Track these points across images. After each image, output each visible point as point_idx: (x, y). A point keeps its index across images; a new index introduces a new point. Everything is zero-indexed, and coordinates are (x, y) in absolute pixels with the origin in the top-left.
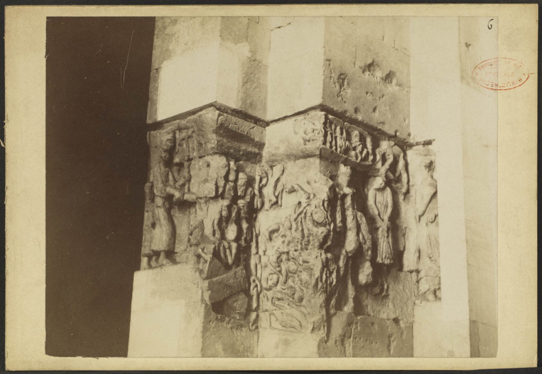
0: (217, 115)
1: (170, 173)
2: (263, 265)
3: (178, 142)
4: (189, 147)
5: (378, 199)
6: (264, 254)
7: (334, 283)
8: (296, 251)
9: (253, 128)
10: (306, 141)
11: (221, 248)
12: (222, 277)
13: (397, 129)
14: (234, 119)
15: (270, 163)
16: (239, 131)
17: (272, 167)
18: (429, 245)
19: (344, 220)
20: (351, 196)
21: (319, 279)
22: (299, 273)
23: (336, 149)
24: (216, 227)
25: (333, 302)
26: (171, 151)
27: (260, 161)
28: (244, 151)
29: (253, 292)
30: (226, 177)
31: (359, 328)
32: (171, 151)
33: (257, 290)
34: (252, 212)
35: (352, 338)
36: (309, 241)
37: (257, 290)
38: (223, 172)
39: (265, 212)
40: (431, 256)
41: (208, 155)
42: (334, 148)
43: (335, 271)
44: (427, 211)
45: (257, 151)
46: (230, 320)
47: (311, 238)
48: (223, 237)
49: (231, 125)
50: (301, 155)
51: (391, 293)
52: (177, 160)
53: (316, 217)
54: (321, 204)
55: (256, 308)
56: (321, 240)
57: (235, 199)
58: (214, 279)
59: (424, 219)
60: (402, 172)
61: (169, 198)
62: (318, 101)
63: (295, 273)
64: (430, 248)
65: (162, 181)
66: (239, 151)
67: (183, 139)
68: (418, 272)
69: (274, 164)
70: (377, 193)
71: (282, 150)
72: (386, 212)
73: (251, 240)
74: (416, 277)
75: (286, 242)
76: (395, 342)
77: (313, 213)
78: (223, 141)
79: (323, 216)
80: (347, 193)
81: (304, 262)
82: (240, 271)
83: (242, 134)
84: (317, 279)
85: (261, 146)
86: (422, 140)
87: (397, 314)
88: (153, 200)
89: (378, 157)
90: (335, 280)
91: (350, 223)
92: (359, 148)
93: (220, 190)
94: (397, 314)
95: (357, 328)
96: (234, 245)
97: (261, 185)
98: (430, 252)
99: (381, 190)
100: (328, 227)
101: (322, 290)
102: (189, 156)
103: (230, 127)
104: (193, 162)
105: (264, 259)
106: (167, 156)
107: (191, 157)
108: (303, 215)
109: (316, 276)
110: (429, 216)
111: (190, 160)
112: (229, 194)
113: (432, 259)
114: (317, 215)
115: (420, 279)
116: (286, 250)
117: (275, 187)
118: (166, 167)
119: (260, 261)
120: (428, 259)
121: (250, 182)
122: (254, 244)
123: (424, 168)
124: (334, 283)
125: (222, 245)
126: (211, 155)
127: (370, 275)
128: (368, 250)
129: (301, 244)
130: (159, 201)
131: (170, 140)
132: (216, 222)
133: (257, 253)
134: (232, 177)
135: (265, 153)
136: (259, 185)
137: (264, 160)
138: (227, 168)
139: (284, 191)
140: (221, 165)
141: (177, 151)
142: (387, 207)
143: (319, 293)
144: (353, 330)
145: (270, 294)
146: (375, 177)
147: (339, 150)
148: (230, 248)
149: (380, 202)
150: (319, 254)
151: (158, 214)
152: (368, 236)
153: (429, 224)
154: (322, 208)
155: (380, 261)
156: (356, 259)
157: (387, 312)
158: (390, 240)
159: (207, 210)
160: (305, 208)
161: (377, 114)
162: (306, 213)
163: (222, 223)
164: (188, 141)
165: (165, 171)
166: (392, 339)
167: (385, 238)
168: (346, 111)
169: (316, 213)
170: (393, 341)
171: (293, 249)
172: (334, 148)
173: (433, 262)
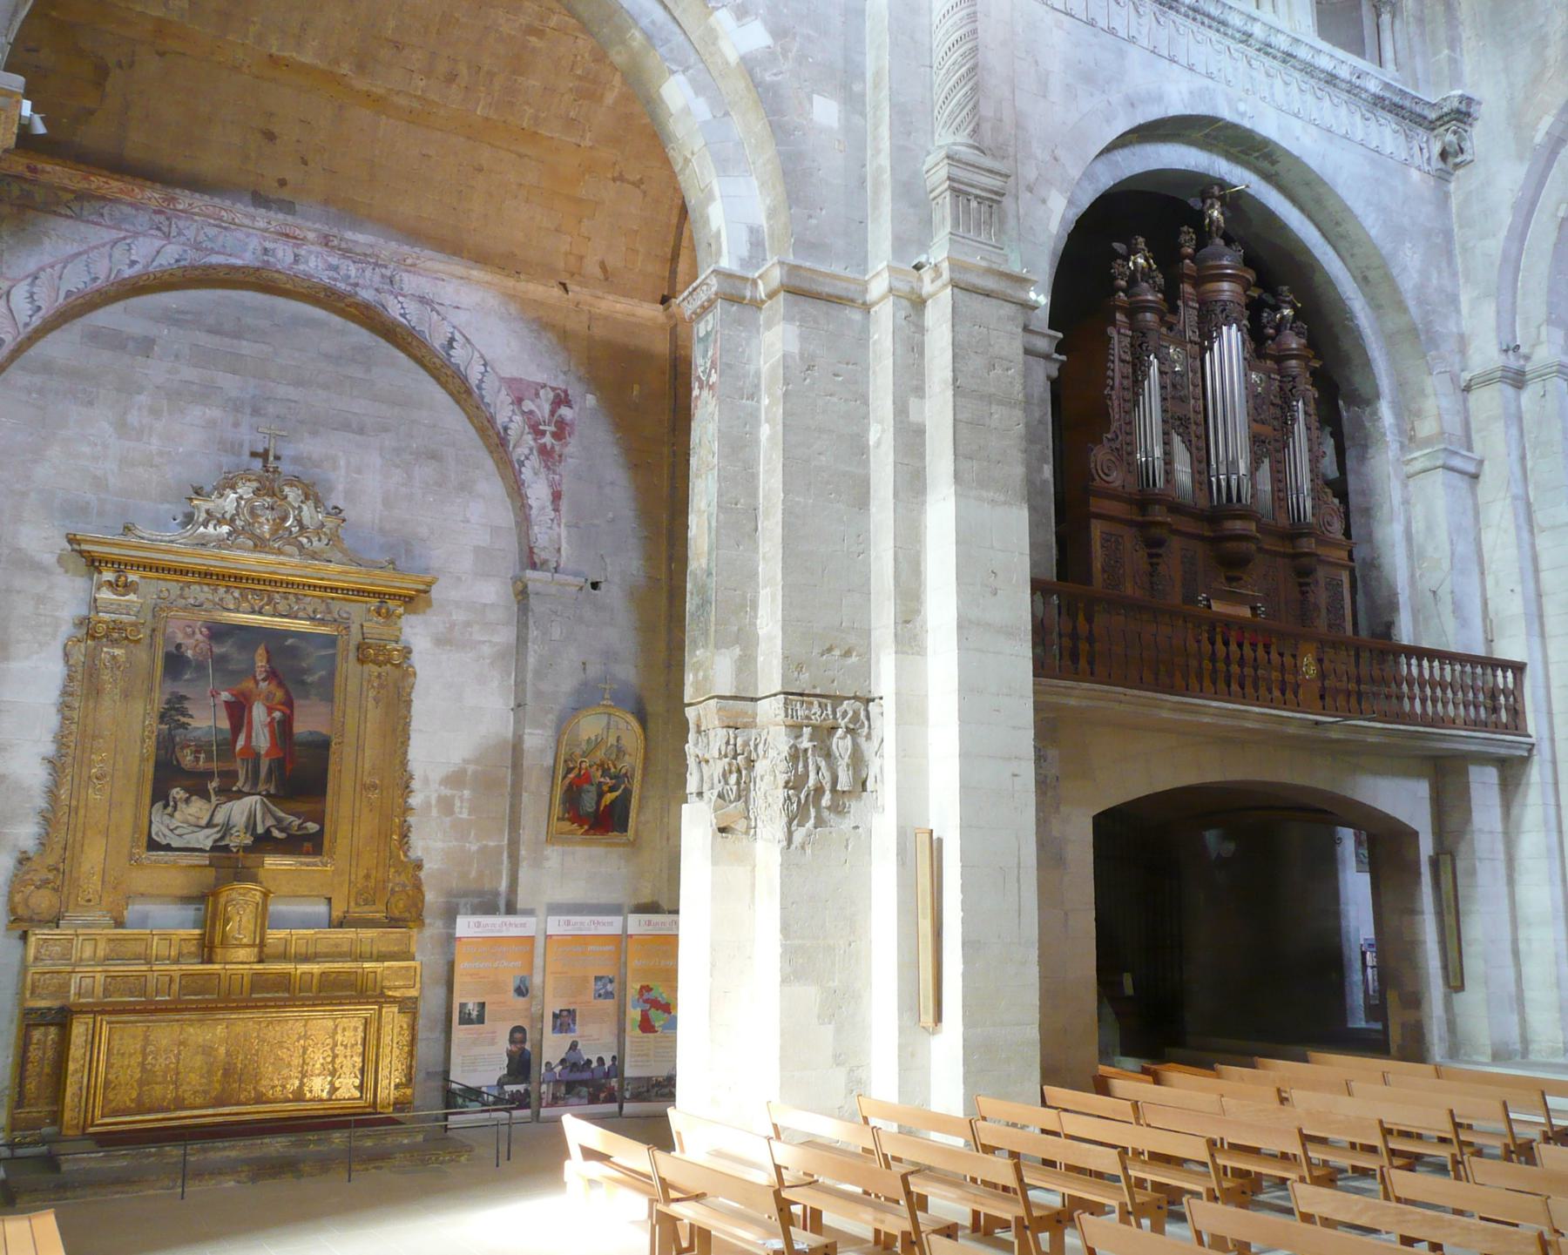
5: (841, 744)
19: (806, 766)
30: (728, 743)
34: (751, 763)
57: (735, 757)
62: (778, 689)
82: (740, 804)
91: (812, 768)
99: (844, 737)
112: (731, 754)
121: (746, 744)
152: (827, 775)
156: (819, 790)
157: (846, 824)
163: (725, 776)
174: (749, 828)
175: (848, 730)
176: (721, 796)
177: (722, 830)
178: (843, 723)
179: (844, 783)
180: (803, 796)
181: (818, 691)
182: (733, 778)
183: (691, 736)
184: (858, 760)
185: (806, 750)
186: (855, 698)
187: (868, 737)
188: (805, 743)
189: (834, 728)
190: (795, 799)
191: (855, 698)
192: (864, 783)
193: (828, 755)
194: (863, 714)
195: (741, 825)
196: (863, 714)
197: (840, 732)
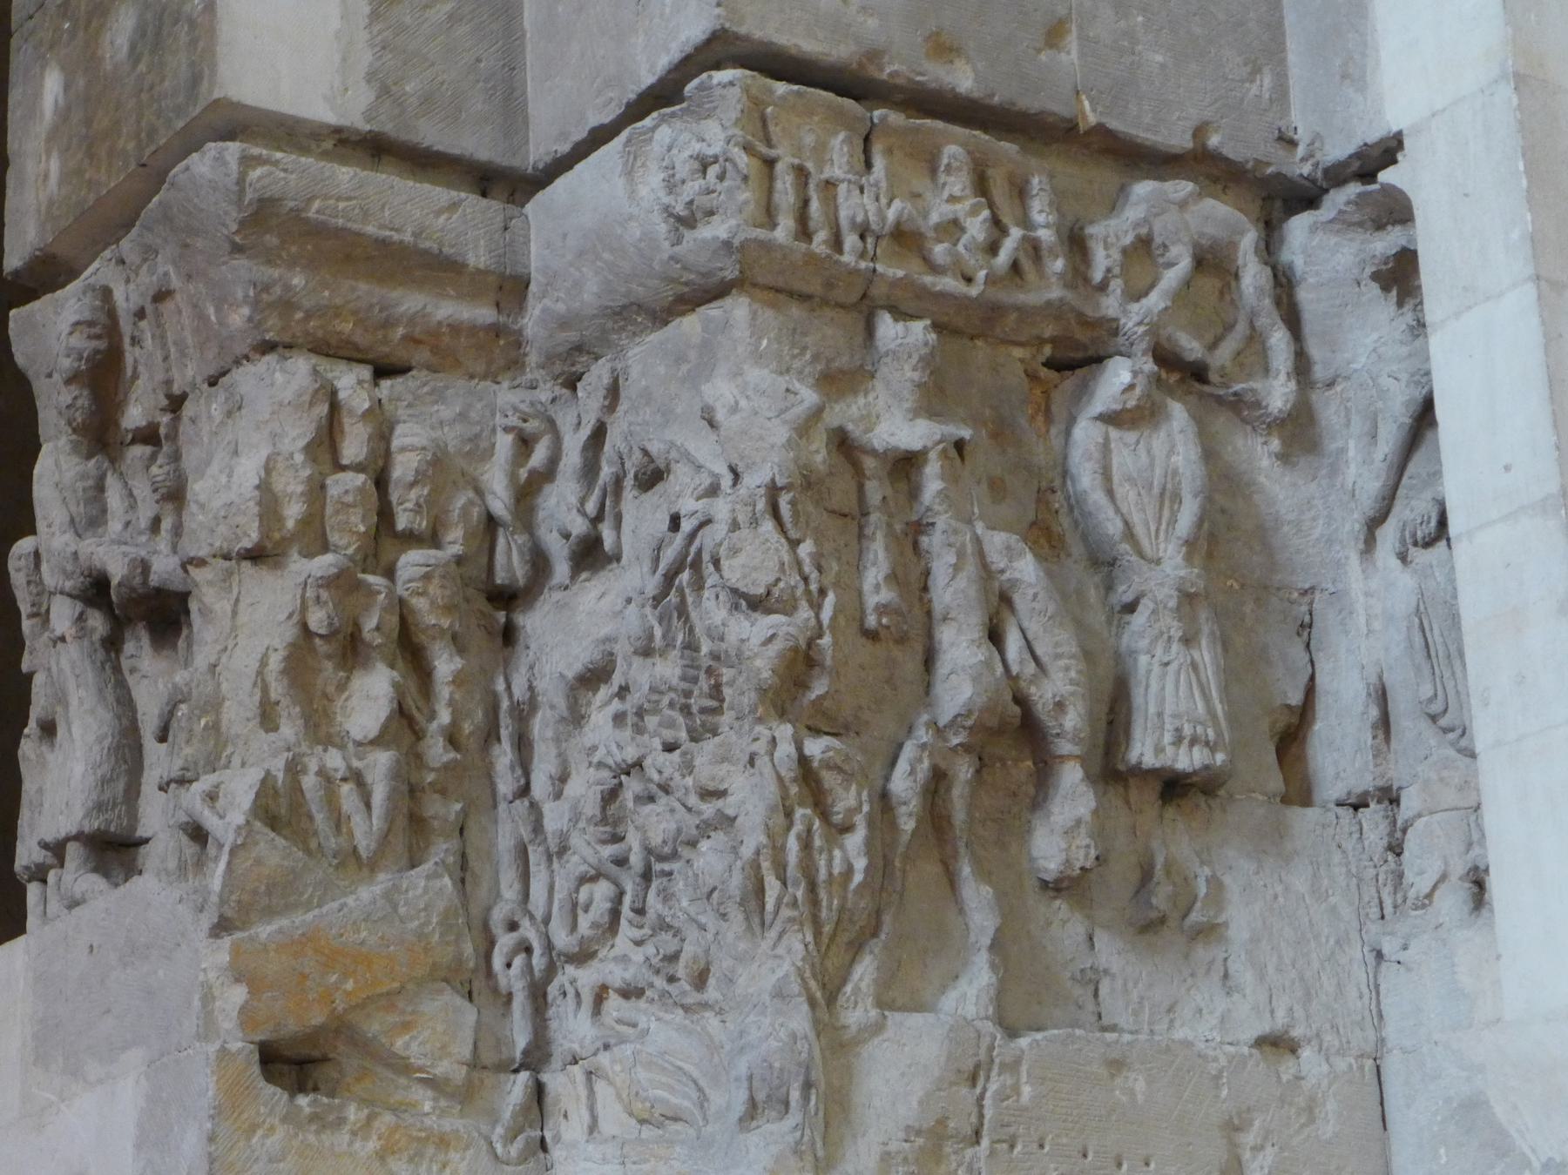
0: (234, 166)
1: (111, 481)
2: (553, 845)
3: (126, 327)
4: (164, 345)
6: (558, 795)
7: (858, 878)
8: (670, 748)
9: (454, 206)
10: (686, 221)
11: (309, 782)
12: (310, 916)
13: (1208, 115)
14: (345, 175)
15: (558, 368)
16: (370, 229)
17: (572, 383)
18: (1420, 656)
20: (944, 454)
21: (766, 865)
22: (685, 852)
23: (837, 243)
24: (277, 690)
25: (865, 971)
26: (103, 374)
27: (515, 364)
28: (412, 320)
29: (513, 979)
31: (1026, 1090)
32: (103, 374)
33: (529, 966)
35: (985, 1142)
36: (716, 691)
37: (529, 966)
38: (298, 434)
39: (557, 595)
40: (1436, 707)
41: (237, 363)
42: (821, 236)
43: (860, 821)
44: (1401, 492)
45: (484, 314)
46: (370, 1118)
47: (727, 674)
48: (320, 726)
49: (316, 204)
50: (668, 294)
51: (1240, 919)
52: (134, 416)
53: (733, 571)
54: (761, 505)
55: (526, 1053)
56: (766, 674)
58: (264, 931)
59: (1388, 535)
60: (1262, 322)
61: (96, 590)
63: (674, 855)
64: (1426, 671)
65: (72, 521)
66: (388, 324)
67: (140, 314)
68: (1390, 797)
69: (578, 368)
70: (1114, 433)
71: (591, 293)
72: (1173, 521)
73: (491, 734)
74: (1384, 827)
75: (630, 719)
76: (1270, 1151)
77: (723, 552)
78: (288, 288)
79: (773, 564)
80: (917, 445)
81: (708, 794)
82: (427, 887)
83: (383, 243)
84: (755, 866)
85: (512, 288)
86: (1337, 150)
87: (1281, 1014)
88: (43, 617)
89: (1102, 261)
90: (860, 864)
91: (952, 590)
92: (976, 228)
93: (293, 512)
94: (1281, 1014)
95: (1016, 1089)
96: (380, 764)
97: (523, 474)
98: (1427, 691)
100: (804, 613)
101: (786, 912)
102: (168, 382)
103: (311, 214)
104: (188, 410)
105: (555, 818)
106: (84, 402)
107: (176, 389)
108: (685, 576)
109: (747, 851)
110: (1412, 510)
111: (176, 403)
112: (349, 528)
113: (1444, 722)
114: (741, 559)
115: (1404, 831)
116: (631, 754)
117: (590, 470)
118: (89, 457)
119: (538, 828)
120: (1424, 725)
122: (504, 756)
123: (1375, 289)
124: (858, 878)
125: (313, 766)
126: (247, 358)
127: (1083, 830)
128: (1060, 706)
129: (686, 710)
130: (63, 614)
131: (91, 324)
132: (275, 662)
133: (525, 791)
134: (354, 446)
135: (532, 322)
136: (513, 476)
137: (533, 359)
138: (323, 409)
139: (629, 482)
140: (288, 395)
141: (129, 372)
142: (1177, 498)
143: (772, 934)
144: (987, 1102)
145: (586, 977)
146: (1099, 360)
147: (851, 241)
148: (357, 778)
149: (1130, 479)
150: (761, 747)
151: (60, 671)
153: (1413, 551)
154: (768, 526)
155: (1149, 761)
157: (1212, 1016)
158: (1205, 654)
159: (235, 613)
160: (692, 536)
161: (1070, 55)
162: (696, 565)
164: (158, 315)
165: (83, 476)
166: (1249, 1138)
167: (1175, 647)
168: (874, 55)
169: (735, 551)
170: (1258, 1149)
171: (657, 743)
172: (821, 236)
173: (1451, 736)
174: (486, 1065)
175: (1180, 372)
176: (278, 810)
177: (291, 1063)
178: (1134, 317)
179: (1176, 714)
180: (903, 783)
181: (963, 79)
182: (369, 697)
183: (56, 471)
184: (1244, 583)
185: (906, 465)
186: (1206, 166)
187: (1299, 432)
188: (896, 426)
189: (1076, 356)
190: (847, 799)
191: (1206, 166)
192: (1291, 736)
193: (1051, 525)
194: (1253, 277)
195: (439, 1032)
196: (1253, 277)
197: (1119, 378)
